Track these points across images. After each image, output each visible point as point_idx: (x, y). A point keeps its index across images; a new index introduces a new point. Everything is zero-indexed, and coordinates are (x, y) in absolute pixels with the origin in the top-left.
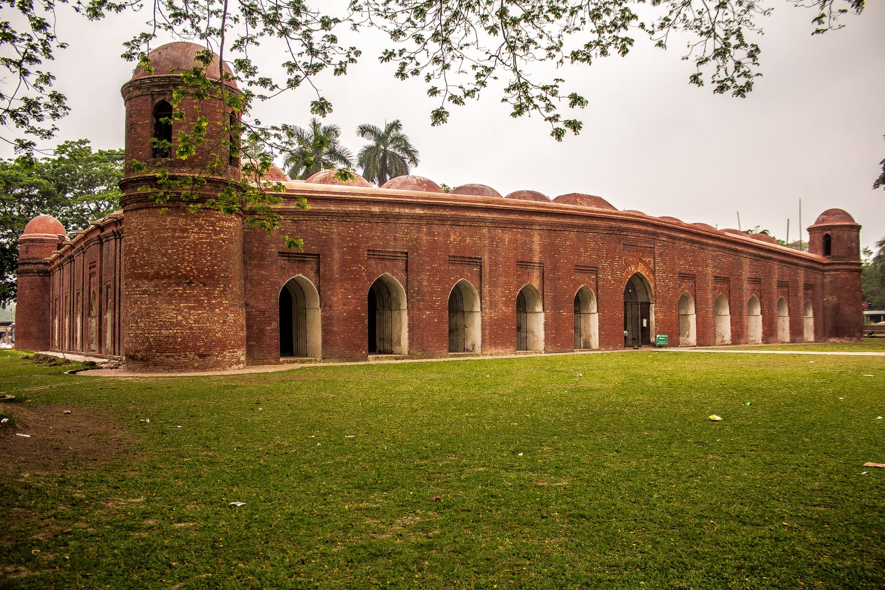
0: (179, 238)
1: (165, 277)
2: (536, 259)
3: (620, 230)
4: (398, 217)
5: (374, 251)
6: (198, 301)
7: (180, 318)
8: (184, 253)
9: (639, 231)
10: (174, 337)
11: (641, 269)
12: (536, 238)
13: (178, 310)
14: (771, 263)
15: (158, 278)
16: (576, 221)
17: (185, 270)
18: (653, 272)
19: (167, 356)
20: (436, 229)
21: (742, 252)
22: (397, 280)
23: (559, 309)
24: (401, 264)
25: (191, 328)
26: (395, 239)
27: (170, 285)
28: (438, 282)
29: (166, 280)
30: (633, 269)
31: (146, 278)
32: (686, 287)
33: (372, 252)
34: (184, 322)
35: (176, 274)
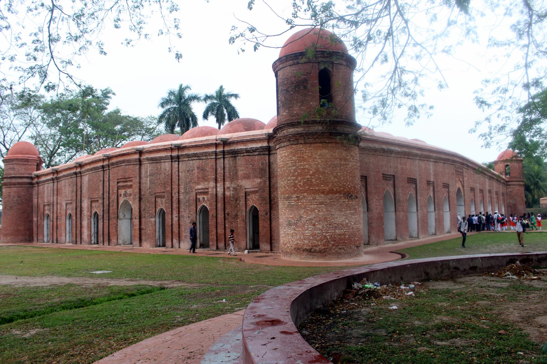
0: (344, 165)
1: (337, 192)
5: (386, 175)
6: (355, 209)
7: (347, 221)
8: (347, 175)
10: (344, 235)
13: (346, 216)
15: (332, 193)
17: (348, 188)
19: (340, 249)
25: (353, 228)
27: (340, 197)
29: (337, 195)
31: (323, 193)
34: (349, 225)
35: (343, 190)
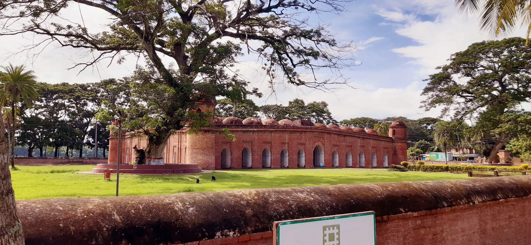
9: (319, 132)
14: (369, 140)
32: (335, 149)
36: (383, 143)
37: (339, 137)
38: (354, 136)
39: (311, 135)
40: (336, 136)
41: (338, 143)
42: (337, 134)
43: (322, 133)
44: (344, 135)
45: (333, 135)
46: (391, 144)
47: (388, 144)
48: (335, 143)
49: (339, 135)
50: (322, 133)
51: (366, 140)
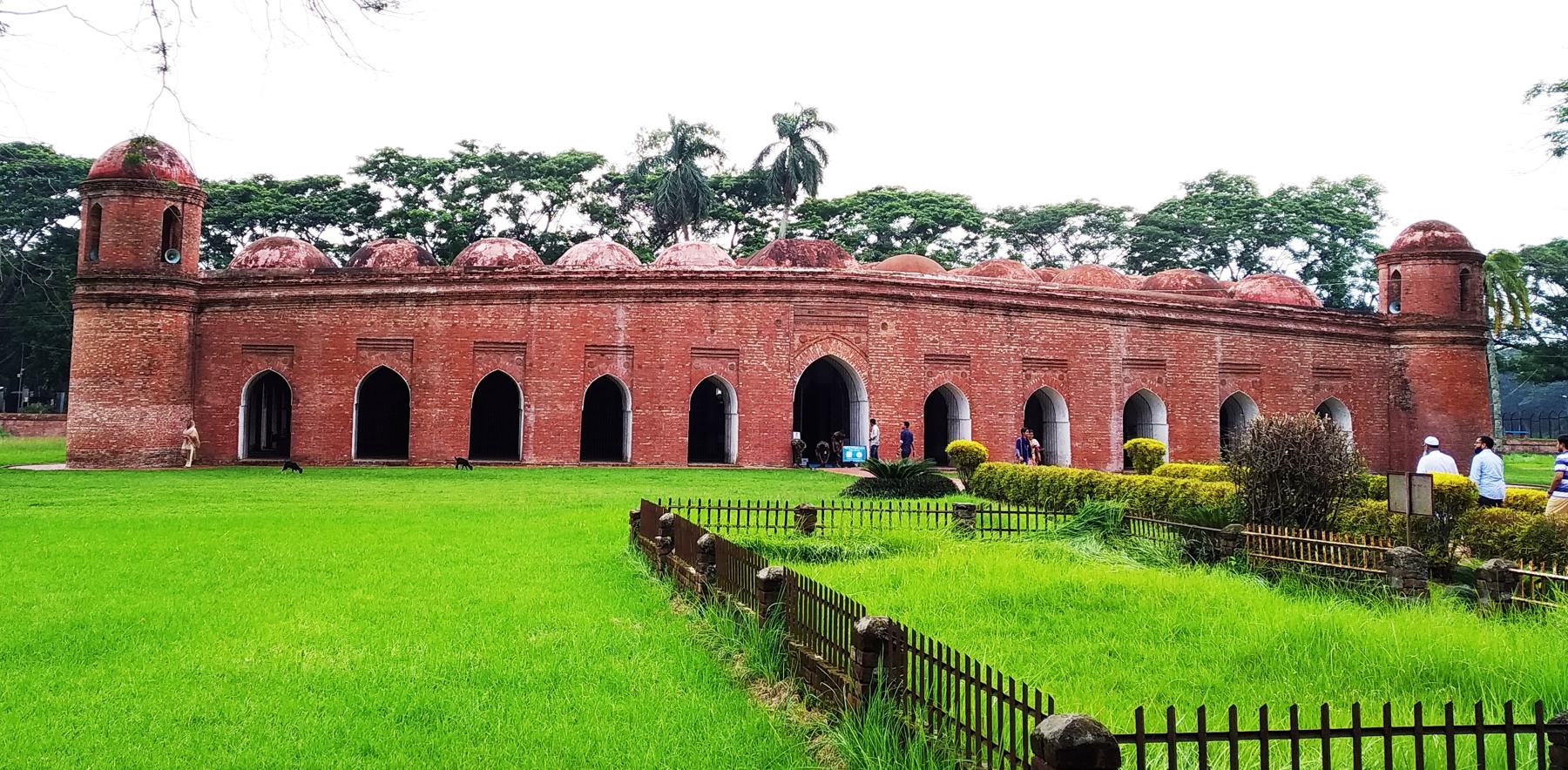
2: (621, 342)
3: (790, 293)
4: (402, 298)
9: (829, 294)
11: (840, 351)
12: (621, 313)
14: (1198, 333)
16: (697, 287)
18: (865, 354)
20: (456, 309)
21: (1103, 315)
22: (402, 369)
23: (661, 408)
24: (405, 354)
26: (396, 324)
28: (457, 374)
30: (817, 352)
33: (363, 343)
36: (1309, 344)
37: (973, 315)
38: (1078, 312)
39: (777, 308)
40: (953, 312)
41: (965, 349)
42: (958, 303)
43: (857, 296)
44: (1007, 308)
45: (924, 309)
46: (1374, 353)
47: (1347, 355)
48: (947, 347)
49: (971, 305)
50: (857, 296)
51: (1170, 330)
